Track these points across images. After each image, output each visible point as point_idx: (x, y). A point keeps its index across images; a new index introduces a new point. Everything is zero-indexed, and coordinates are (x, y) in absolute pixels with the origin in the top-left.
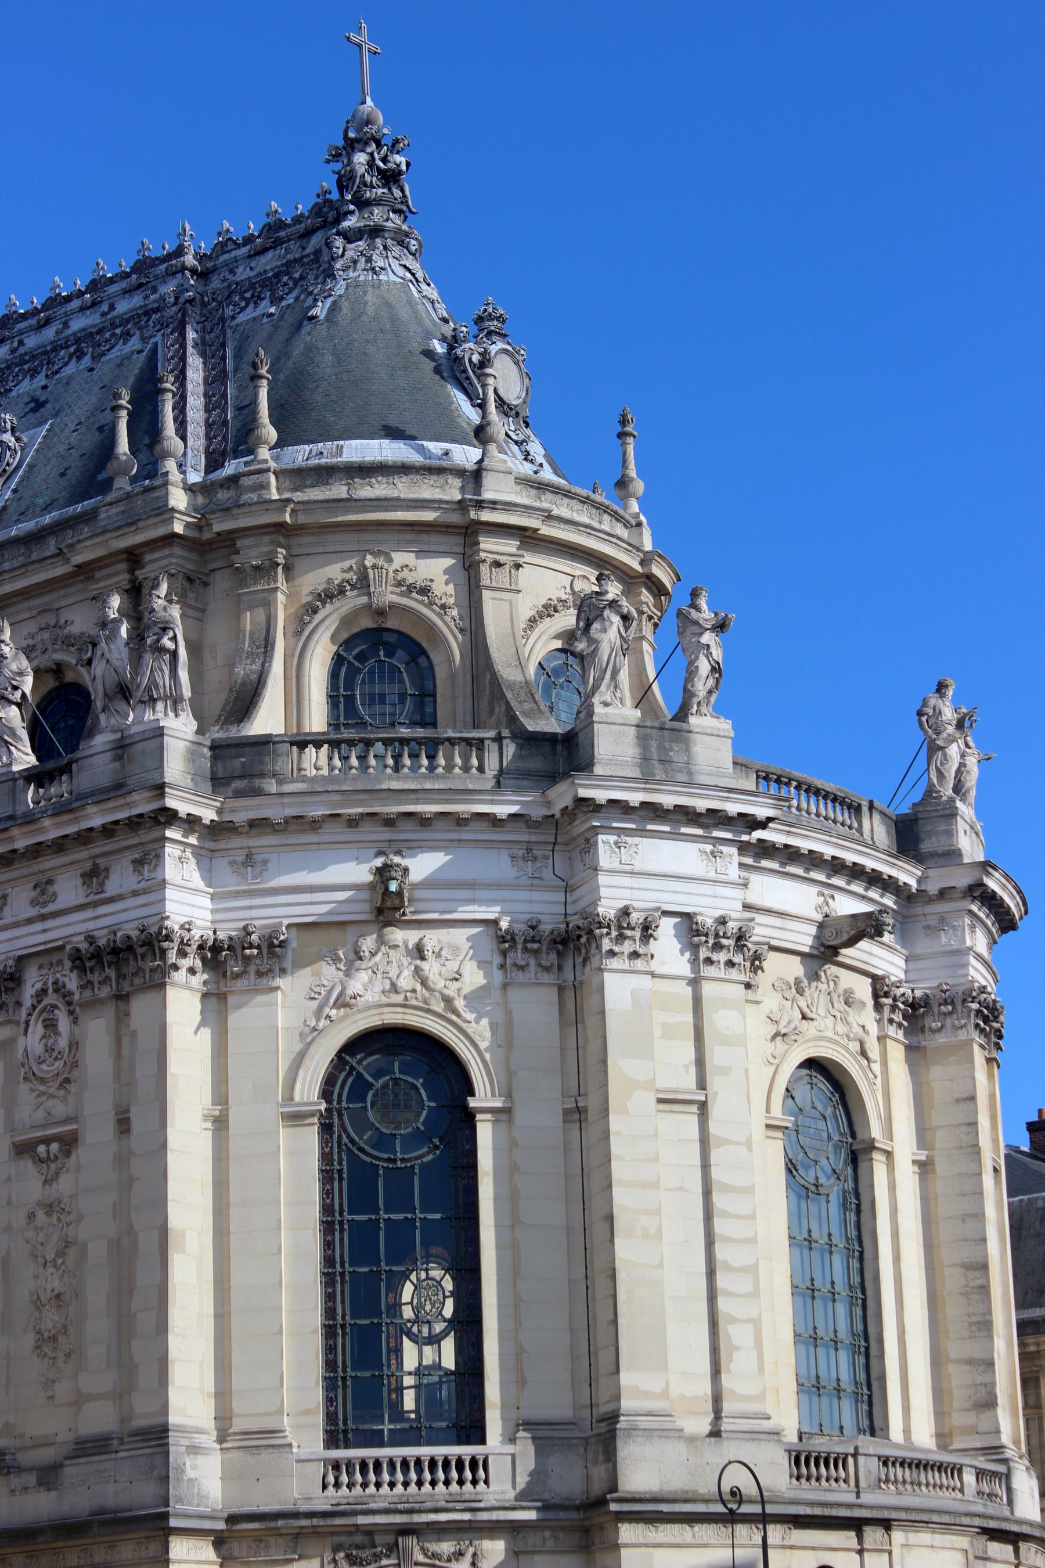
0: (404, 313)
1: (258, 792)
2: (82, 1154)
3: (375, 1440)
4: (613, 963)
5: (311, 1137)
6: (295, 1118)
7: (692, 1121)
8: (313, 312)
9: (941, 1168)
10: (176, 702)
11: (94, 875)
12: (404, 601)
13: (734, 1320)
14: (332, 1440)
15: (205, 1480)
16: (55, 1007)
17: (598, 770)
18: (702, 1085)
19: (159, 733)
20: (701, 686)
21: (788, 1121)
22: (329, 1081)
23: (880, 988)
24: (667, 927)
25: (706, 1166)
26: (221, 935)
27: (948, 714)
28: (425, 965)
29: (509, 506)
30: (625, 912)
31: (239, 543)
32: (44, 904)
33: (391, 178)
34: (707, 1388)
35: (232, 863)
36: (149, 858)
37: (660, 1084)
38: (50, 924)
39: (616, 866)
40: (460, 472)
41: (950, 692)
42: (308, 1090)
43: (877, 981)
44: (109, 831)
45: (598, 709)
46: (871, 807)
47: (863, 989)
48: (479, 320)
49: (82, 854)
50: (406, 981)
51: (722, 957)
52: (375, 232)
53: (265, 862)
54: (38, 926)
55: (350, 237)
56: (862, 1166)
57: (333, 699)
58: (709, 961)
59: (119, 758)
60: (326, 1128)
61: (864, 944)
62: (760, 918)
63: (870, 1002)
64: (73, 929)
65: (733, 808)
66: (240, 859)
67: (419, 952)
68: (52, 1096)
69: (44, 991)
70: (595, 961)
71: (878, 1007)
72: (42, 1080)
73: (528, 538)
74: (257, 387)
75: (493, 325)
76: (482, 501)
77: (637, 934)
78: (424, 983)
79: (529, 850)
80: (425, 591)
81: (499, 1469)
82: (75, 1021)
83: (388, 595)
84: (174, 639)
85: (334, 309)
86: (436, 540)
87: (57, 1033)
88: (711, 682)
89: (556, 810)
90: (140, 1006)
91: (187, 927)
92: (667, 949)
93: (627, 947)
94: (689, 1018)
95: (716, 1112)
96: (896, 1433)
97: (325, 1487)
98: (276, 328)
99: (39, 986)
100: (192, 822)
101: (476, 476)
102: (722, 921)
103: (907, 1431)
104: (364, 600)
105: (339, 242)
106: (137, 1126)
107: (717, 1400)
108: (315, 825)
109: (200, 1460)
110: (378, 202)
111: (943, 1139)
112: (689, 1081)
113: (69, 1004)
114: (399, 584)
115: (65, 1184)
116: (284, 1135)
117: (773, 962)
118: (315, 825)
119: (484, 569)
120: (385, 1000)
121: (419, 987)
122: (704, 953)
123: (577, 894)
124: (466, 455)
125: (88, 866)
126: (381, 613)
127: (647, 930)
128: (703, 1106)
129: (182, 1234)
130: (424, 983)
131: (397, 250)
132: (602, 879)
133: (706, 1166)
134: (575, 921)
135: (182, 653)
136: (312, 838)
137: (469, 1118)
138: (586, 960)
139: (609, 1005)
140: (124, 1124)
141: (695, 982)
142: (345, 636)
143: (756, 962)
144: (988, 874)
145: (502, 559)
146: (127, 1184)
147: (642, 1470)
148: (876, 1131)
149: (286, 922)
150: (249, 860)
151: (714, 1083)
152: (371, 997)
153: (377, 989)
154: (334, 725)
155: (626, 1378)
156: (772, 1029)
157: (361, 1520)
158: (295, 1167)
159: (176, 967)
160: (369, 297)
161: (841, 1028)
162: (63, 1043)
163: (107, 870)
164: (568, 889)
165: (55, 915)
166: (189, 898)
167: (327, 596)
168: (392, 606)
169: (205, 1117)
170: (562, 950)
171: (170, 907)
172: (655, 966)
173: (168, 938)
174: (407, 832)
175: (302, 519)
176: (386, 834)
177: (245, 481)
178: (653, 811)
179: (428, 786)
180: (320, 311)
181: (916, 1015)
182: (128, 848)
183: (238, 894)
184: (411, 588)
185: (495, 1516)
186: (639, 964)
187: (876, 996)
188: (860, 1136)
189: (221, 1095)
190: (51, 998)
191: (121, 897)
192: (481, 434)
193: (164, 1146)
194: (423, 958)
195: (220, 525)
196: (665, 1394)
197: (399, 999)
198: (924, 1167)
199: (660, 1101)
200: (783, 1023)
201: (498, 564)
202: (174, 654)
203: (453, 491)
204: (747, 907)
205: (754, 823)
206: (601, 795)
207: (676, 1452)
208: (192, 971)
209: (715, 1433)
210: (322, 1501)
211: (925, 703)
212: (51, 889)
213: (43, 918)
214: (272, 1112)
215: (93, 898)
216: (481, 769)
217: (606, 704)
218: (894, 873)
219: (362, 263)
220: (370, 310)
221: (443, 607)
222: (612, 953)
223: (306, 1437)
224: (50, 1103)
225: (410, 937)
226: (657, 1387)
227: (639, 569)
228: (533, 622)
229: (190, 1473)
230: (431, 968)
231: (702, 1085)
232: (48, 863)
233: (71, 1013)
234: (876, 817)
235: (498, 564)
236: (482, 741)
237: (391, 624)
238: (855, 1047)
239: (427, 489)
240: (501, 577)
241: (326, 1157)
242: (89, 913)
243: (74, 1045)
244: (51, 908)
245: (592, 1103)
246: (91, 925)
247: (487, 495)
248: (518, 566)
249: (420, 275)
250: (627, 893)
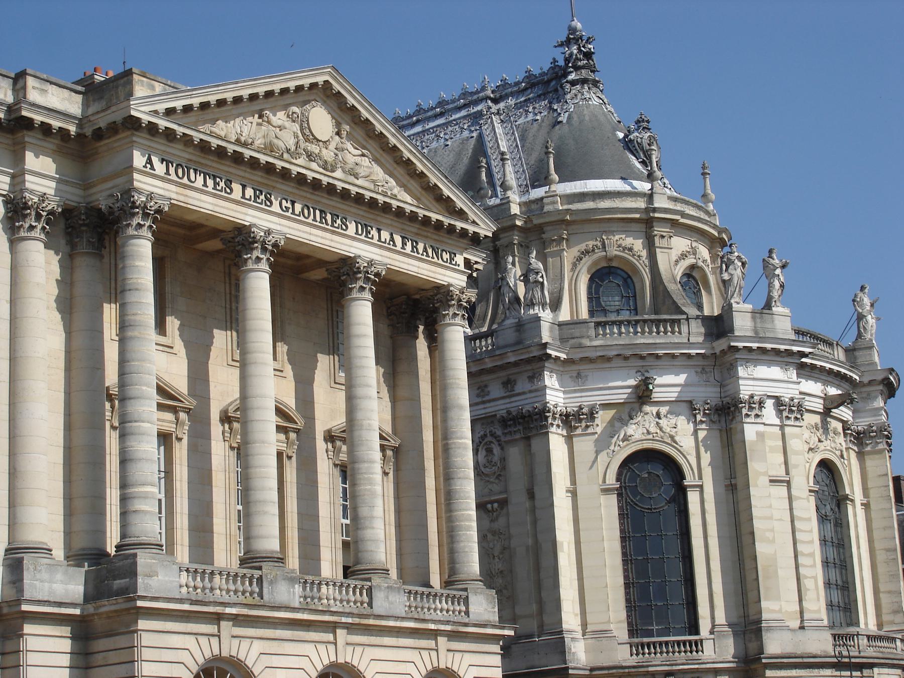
0: (602, 118)
2: (511, 508)
3: (650, 634)
4: (748, 420)
5: (613, 499)
6: (606, 491)
7: (783, 490)
8: (560, 119)
9: (873, 506)
10: (544, 305)
11: (508, 384)
12: (621, 254)
13: (806, 577)
14: (632, 633)
15: (580, 653)
16: (491, 442)
17: (737, 333)
18: (787, 473)
19: (538, 319)
20: (776, 294)
21: (816, 488)
23: (846, 426)
24: (769, 403)
25: (791, 509)
26: (569, 410)
27: (867, 301)
28: (660, 421)
29: (666, 211)
30: (752, 396)
31: (545, 229)
32: (483, 396)
33: (588, 55)
34: (797, 608)
35: (571, 377)
36: (536, 376)
37: (771, 473)
38: (488, 405)
39: (746, 376)
40: (642, 195)
41: (866, 291)
42: (611, 479)
43: (844, 422)
44: (516, 364)
45: (734, 305)
46: (837, 344)
47: (839, 426)
48: (638, 122)
49: (503, 374)
50: (653, 429)
51: (793, 416)
52: (584, 81)
53: (586, 376)
54: (482, 406)
55: (573, 83)
56: (842, 506)
57: (590, 299)
58: (788, 418)
59: (518, 331)
60: (619, 495)
61: (841, 408)
62: (807, 398)
63: (841, 432)
65: (795, 349)
66: (575, 375)
67: (658, 416)
68: (492, 483)
69: (485, 435)
70: (738, 419)
71: (845, 435)
72: (487, 475)
73: (674, 223)
74: (548, 158)
75: (645, 124)
76: (655, 208)
77: (757, 406)
78: (661, 429)
79: (703, 369)
80: (630, 249)
81: (708, 646)
82: (502, 449)
83: (613, 251)
84: (542, 277)
85: (569, 118)
86: (635, 227)
87: (493, 454)
88: (780, 292)
89: (717, 351)
90: (535, 443)
91: (556, 406)
92: (769, 412)
93: (753, 413)
94: (781, 443)
95: (793, 485)
96: (862, 625)
97: (631, 655)
98: (540, 126)
99: (482, 433)
100: (557, 358)
101: (650, 197)
102: (792, 399)
103: (866, 624)
104: (604, 253)
105: (568, 86)
106: (538, 495)
107: (802, 613)
108: (609, 359)
109: (577, 644)
110: (583, 67)
111: (872, 493)
112: (782, 472)
113: (498, 441)
114: (619, 246)
115: (502, 521)
116: (603, 499)
117: (807, 416)
118: (609, 359)
119: (657, 239)
120: (644, 438)
121: (658, 431)
122: (785, 414)
123: (726, 389)
124: (645, 186)
125: (505, 379)
126: (610, 260)
127: (761, 404)
128: (788, 482)
129: (562, 543)
130: (661, 429)
131: (594, 89)
132: (741, 382)
133: (791, 509)
134: (728, 400)
135: (545, 282)
136: (607, 365)
138: (734, 418)
139: (747, 438)
140: (531, 495)
141: (782, 427)
142: (594, 270)
144: (891, 374)
145: (664, 234)
146: (535, 522)
147: (774, 645)
148: (848, 491)
149: (599, 403)
150: (579, 376)
151: (793, 472)
152: (638, 436)
153: (640, 433)
154: (591, 313)
155: (764, 604)
156: (806, 447)
157: (651, 669)
158: (606, 514)
159: (552, 425)
160: (585, 112)
161: (833, 445)
162: (496, 459)
163: (515, 381)
164: (722, 386)
165: (489, 401)
166: (556, 394)
167: (586, 252)
168: (616, 256)
169: (567, 491)
170: (724, 415)
171: (548, 398)
172: (764, 420)
173: (549, 411)
174: (651, 362)
175: (574, 218)
176: (640, 363)
177: (545, 200)
178: (763, 350)
179: (658, 341)
180: (563, 118)
181: (860, 438)
182: (526, 371)
183: (575, 391)
184: (624, 248)
185: (708, 666)
186: (759, 420)
187: (844, 430)
188: (841, 493)
189: (573, 481)
190: (489, 438)
191: (524, 393)
192: (650, 177)
193: (552, 505)
194: (660, 418)
195: (536, 221)
196: (780, 611)
197: (650, 437)
198: (866, 506)
199: (771, 481)
200: (811, 443)
201: (663, 237)
202: (542, 284)
203: (641, 204)
204: (801, 393)
205: (803, 355)
206: (740, 345)
207: (787, 635)
208: (558, 426)
209: (802, 628)
210: (633, 661)
211: (856, 296)
212: (486, 390)
213: (484, 402)
214: (596, 489)
215: (508, 394)
216: (680, 333)
217: (738, 303)
218: (851, 374)
219: (579, 96)
220: (587, 118)
221: (639, 256)
222: (747, 416)
223: (621, 631)
224: (490, 486)
225: (654, 410)
226: (777, 608)
227: (716, 234)
228: (677, 261)
229: (573, 650)
230: (663, 422)
231: (787, 473)
232: (485, 378)
233: (499, 445)
234: (840, 348)
235: (663, 237)
236: (679, 320)
237: (614, 264)
238: (838, 453)
239: (629, 203)
240: (664, 243)
241: (620, 508)
242: (507, 400)
243: (503, 459)
244: (487, 398)
245: (740, 482)
246: (508, 406)
247: (656, 205)
248: (671, 237)
249: (605, 100)
250: (751, 388)
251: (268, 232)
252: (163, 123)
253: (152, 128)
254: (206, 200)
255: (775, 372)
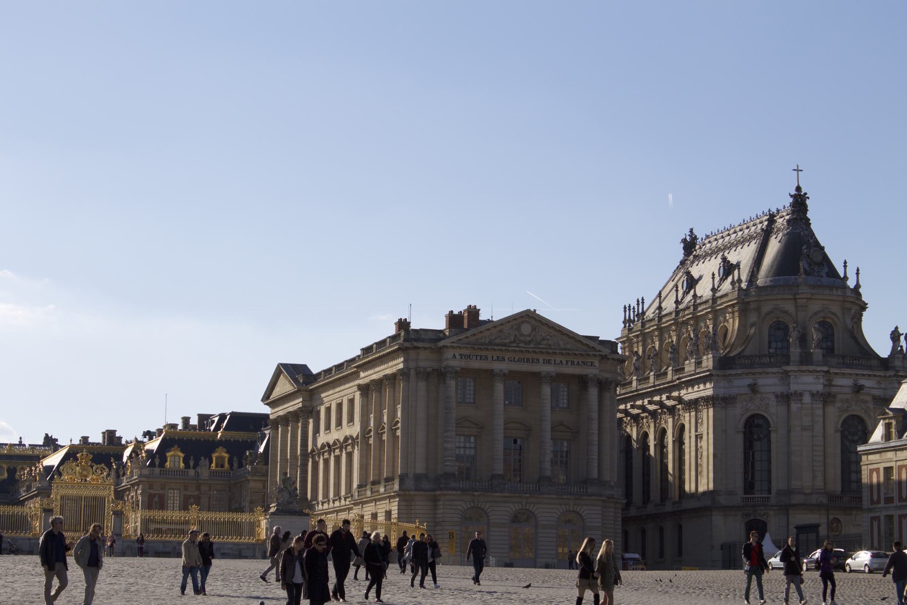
1: (731, 368)
14: (745, 494)
22: (746, 424)
47: (869, 398)
64: (703, 394)
92: (807, 399)
108: (740, 375)
117: (839, 397)
127: (801, 394)
137: (770, 431)
143: (834, 396)
251: (501, 370)
252: (455, 345)
253: (453, 347)
254: (476, 364)
255: (809, 379)
